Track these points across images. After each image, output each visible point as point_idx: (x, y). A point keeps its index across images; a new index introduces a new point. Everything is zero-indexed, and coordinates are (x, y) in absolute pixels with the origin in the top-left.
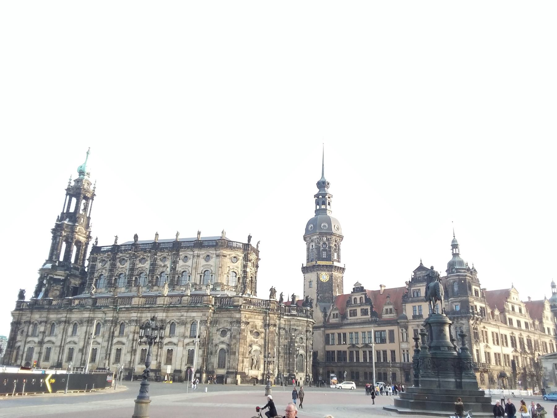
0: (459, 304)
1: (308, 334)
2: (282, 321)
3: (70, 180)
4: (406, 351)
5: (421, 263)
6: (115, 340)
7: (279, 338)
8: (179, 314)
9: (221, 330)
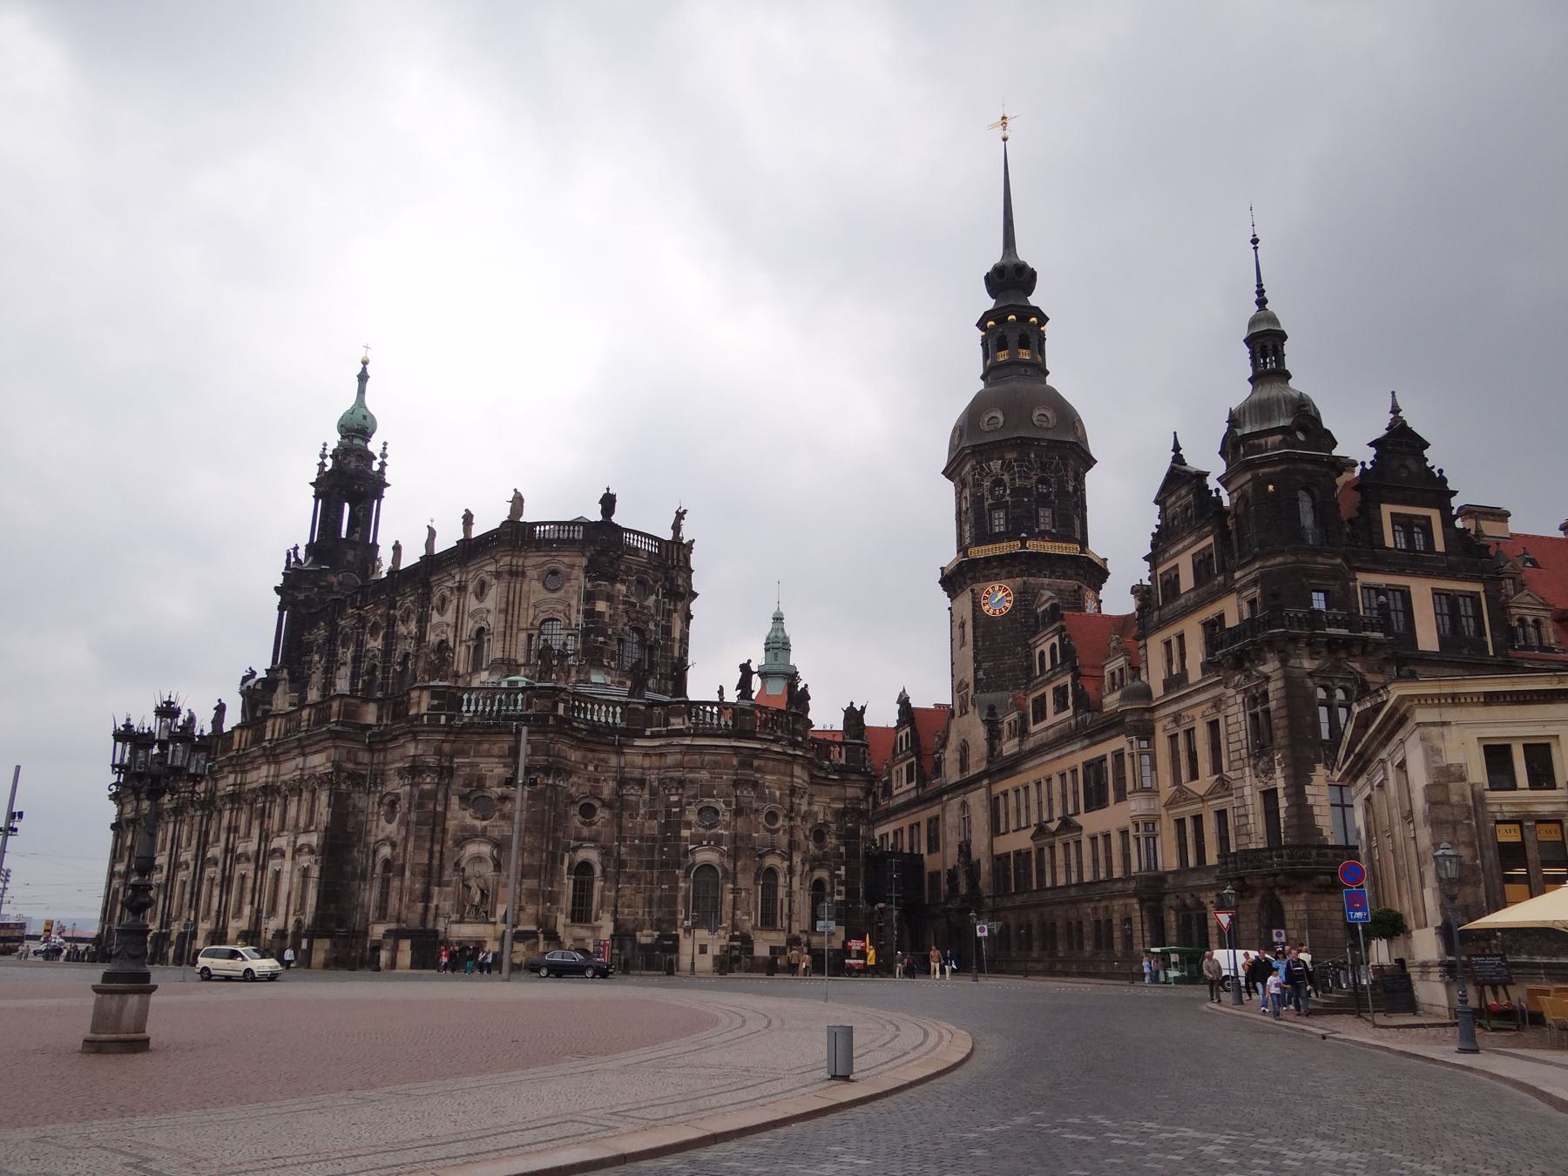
0: (1255, 592)
1: (747, 793)
2: (635, 759)
3: (323, 456)
4: (1141, 827)
5: (1178, 459)
6: (209, 855)
7: (620, 816)
8: (294, 763)
9: (386, 801)
